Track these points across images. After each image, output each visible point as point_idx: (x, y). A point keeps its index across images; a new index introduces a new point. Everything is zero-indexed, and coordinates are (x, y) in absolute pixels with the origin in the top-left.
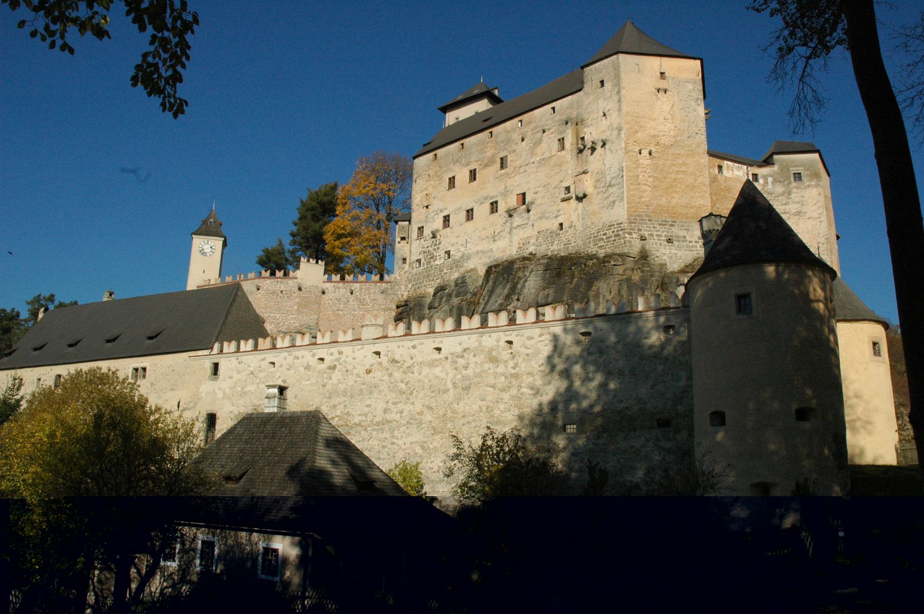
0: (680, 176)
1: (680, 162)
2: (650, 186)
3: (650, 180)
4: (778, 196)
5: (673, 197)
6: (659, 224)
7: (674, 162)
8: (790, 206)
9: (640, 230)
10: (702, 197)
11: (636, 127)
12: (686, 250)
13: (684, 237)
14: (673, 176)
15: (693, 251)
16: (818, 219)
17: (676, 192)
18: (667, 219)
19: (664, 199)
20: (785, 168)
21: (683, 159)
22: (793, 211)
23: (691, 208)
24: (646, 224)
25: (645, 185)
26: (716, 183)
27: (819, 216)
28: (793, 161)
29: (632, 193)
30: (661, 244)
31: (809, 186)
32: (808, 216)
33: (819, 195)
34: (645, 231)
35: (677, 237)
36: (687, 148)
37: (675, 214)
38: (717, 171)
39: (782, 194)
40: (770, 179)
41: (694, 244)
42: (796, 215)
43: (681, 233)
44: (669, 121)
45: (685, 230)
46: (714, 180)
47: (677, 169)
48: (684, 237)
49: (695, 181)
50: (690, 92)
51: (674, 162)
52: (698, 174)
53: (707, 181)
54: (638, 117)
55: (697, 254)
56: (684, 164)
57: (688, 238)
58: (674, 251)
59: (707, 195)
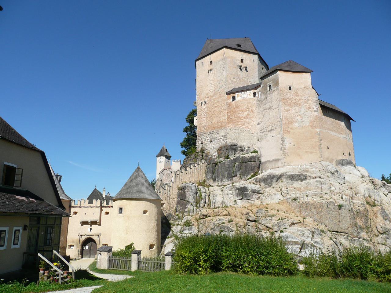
0: (217, 108)
1: (216, 102)
2: (205, 118)
3: (205, 115)
4: (263, 101)
5: (213, 120)
6: (208, 134)
7: (214, 103)
8: (267, 105)
9: (201, 139)
10: (224, 116)
11: (201, 92)
12: (217, 144)
13: (217, 137)
14: (213, 110)
15: (219, 143)
16: (278, 109)
17: (214, 117)
18: (211, 131)
19: (210, 122)
20: (265, 85)
21: (217, 100)
22: (268, 107)
23: (220, 122)
24: (204, 136)
25: (203, 118)
26: (231, 106)
27: (278, 106)
28: (268, 80)
29: (199, 123)
30: (208, 144)
31: (274, 91)
32: (273, 108)
33: (278, 94)
34: (203, 139)
35: (214, 138)
36: (219, 94)
37: (213, 127)
38: (231, 100)
39: (264, 100)
40: (260, 93)
41: (220, 140)
42: (269, 109)
43: (215, 136)
44: (213, 84)
45: (217, 134)
46: (230, 105)
47: (215, 106)
48: (217, 137)
49: (221, 108)
50: (221, 66)
51: (214, 103)
52: (222, 105)
53: (225, 107)
54: (202, 87)
55: (221, 144)
56: (218, 102)
57: (218, 138)
58: (213, 145)
59: (226, 114)
